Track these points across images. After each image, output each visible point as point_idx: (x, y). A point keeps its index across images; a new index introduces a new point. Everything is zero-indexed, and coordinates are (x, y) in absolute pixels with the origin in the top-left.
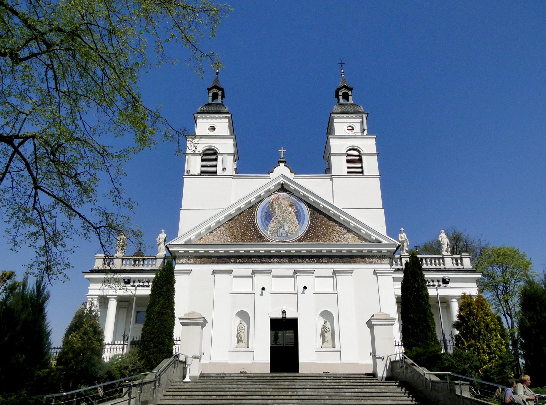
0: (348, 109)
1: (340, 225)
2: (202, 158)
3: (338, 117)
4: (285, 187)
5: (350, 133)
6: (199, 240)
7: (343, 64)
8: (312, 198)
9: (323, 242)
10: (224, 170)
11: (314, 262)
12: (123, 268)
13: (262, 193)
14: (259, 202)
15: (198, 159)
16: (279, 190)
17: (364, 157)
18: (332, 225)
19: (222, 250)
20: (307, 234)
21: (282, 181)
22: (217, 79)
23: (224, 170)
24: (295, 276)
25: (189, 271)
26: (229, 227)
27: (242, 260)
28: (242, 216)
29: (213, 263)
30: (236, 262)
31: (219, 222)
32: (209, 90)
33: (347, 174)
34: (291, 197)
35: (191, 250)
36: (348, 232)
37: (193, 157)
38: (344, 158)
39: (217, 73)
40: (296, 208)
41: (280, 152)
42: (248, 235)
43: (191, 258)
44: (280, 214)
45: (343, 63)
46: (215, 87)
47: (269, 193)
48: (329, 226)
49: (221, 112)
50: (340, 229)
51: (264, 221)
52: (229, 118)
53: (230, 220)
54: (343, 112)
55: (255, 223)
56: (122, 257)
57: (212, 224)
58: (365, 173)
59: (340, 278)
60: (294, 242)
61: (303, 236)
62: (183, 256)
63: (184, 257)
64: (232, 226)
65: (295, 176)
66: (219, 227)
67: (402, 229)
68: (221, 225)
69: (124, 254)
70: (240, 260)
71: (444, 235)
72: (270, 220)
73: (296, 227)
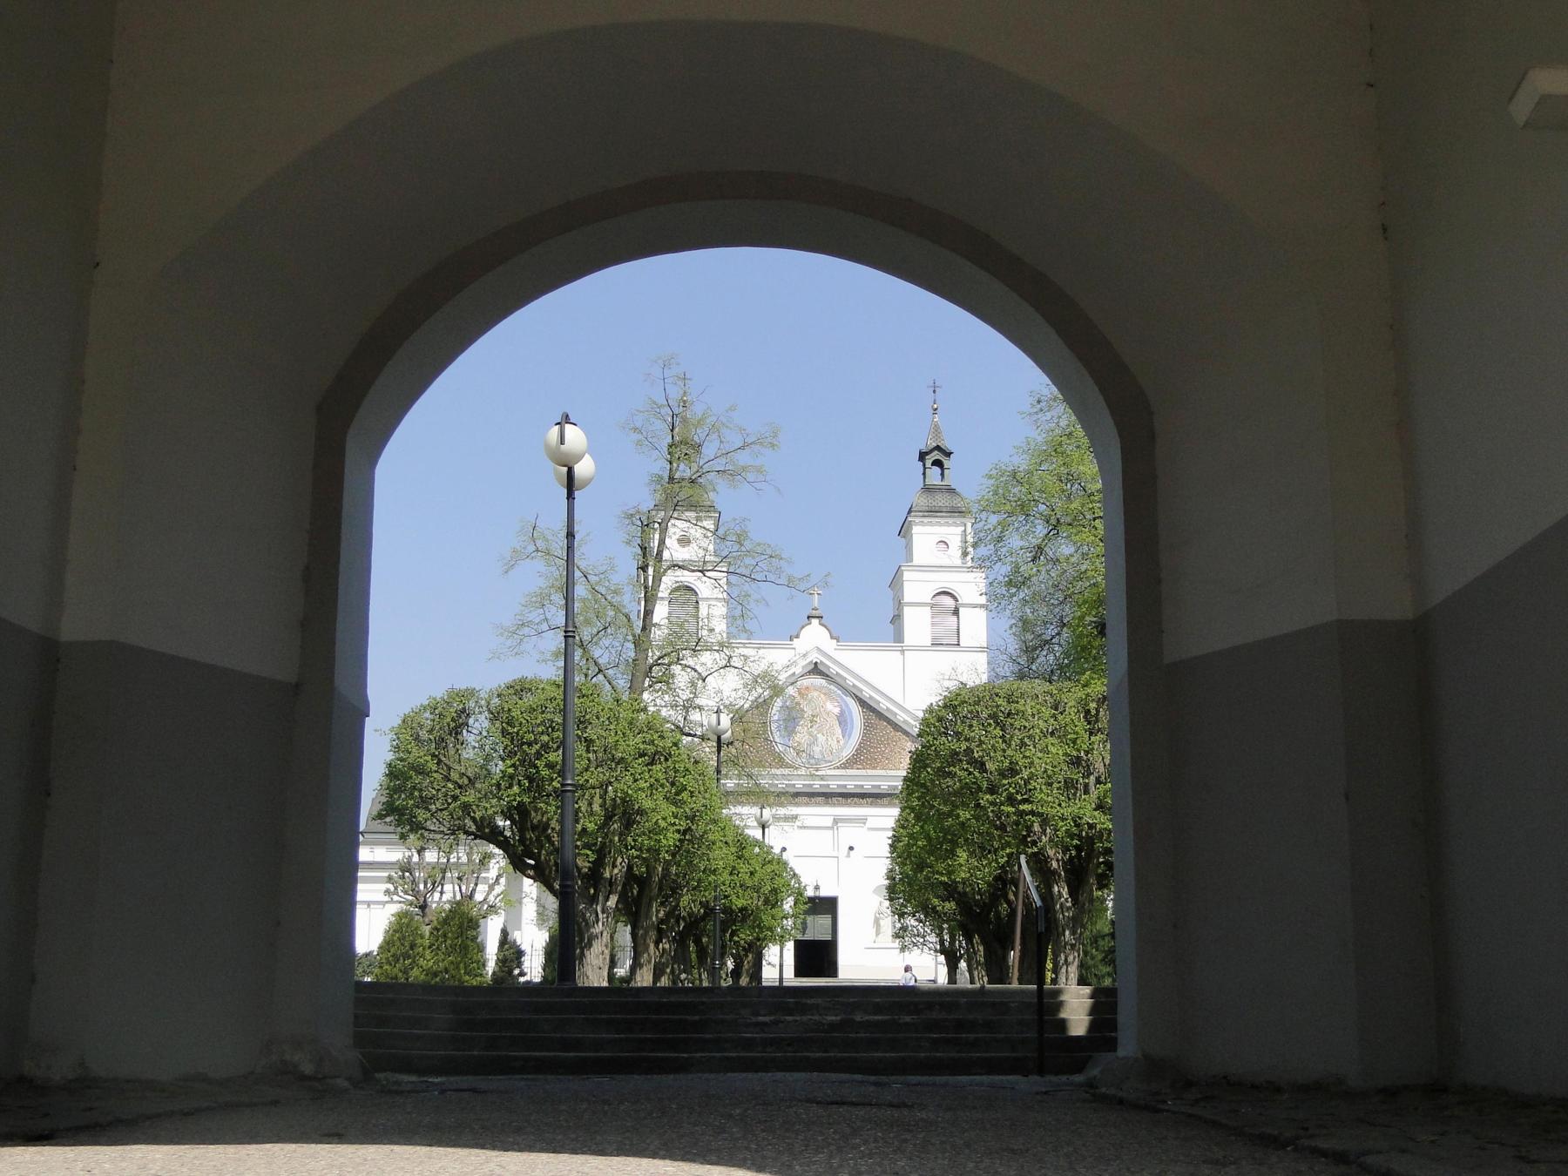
0: (940, 504)
7: (936, 389)
11: (867, 803)
34: (832, 687)
61: (849, 759)
73: (838, 742)
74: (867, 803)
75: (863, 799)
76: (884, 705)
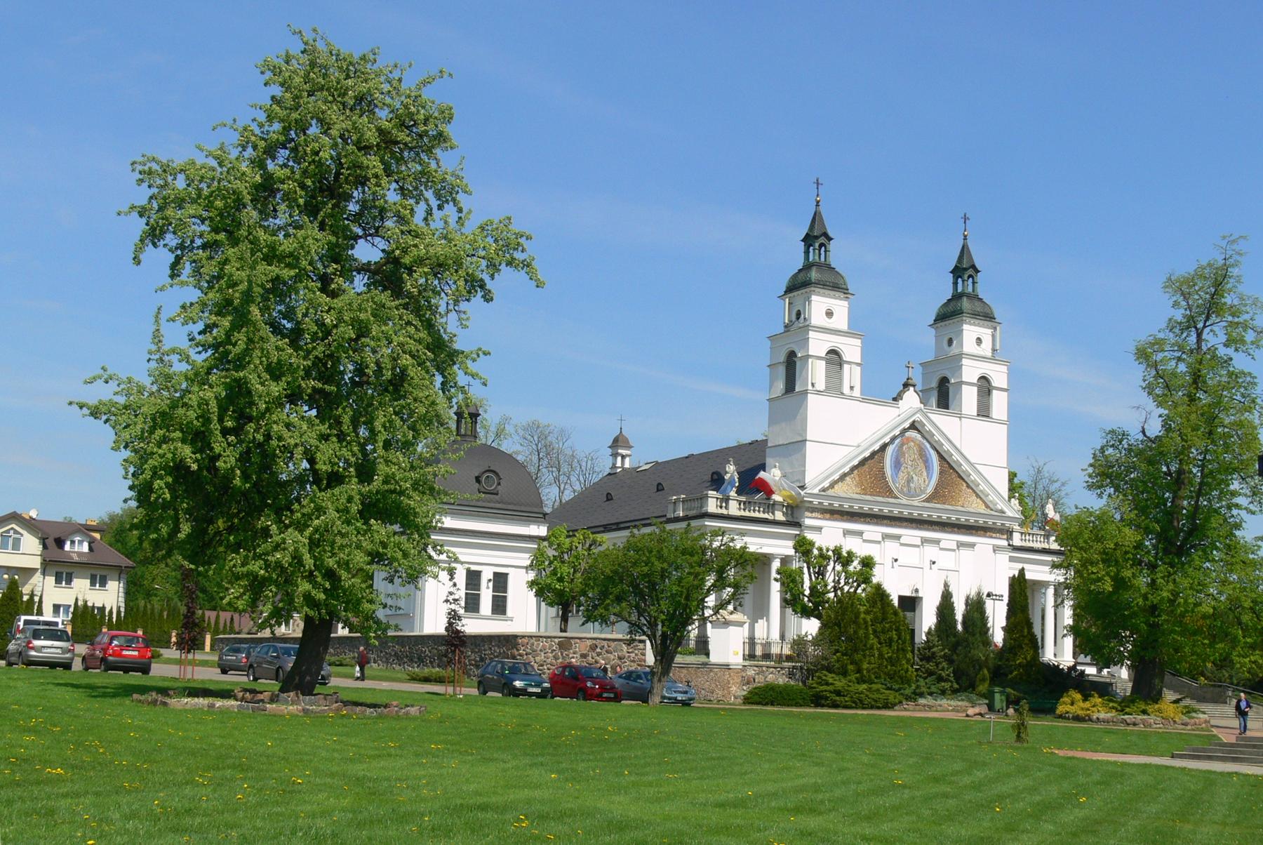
4: (916, 424)
8: (947, 446)
10: (852, 388)
17: (995, 393)
23: (852, 388)
38: (975, 389)
59: (964, 552)
76: (956, 456)
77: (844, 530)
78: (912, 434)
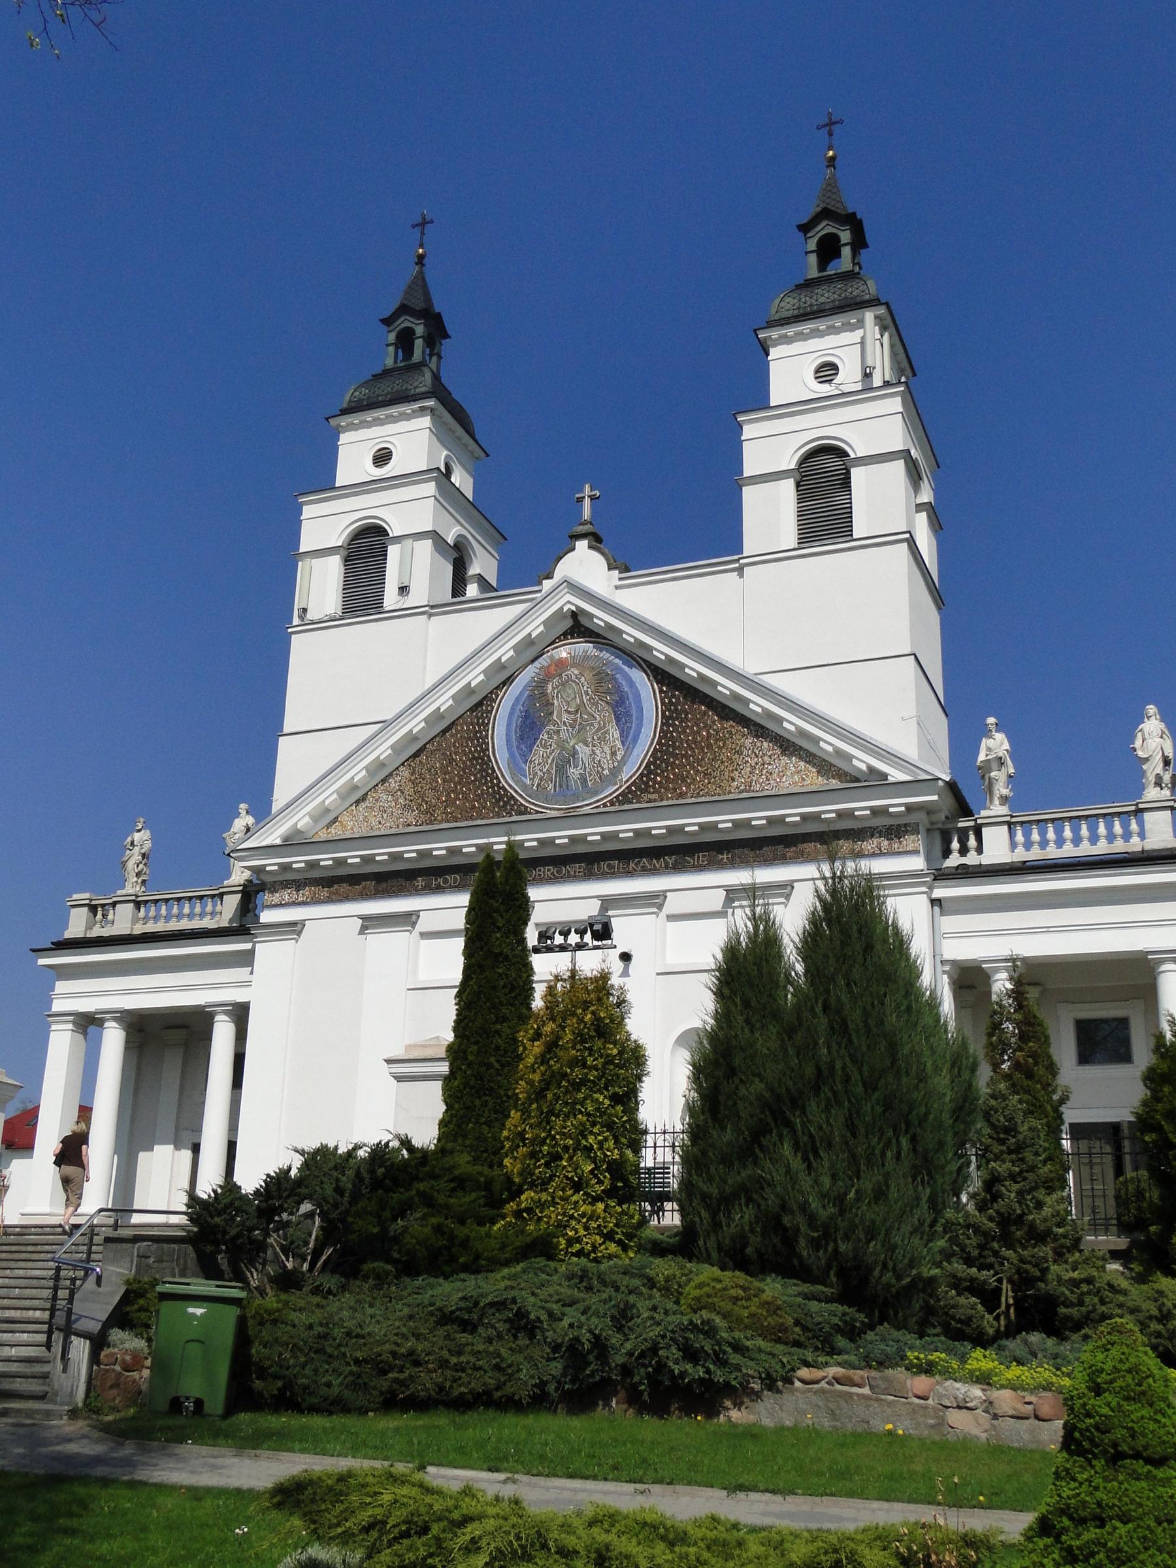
0: (822, 300)
1: (758, 729)
2: (346, 561)
3: (781, 337)
4: (583, 621)
5: (825, 389)
6: (328, 826)
8: (661, 650)
9: (698, 795)
10: (403, 590)
11: (667, 867)
12: (139, 929)
13: (505, 652)
14: (504, 683)
15: (334, 566)
16: (565, 635)
17: (857, 474)
18: (730, 733)
19: (381, 854)
20: (647, 776)
21: (569, 602)
22: (831, 187)
23: (403, 590)
24: (730, 911)
25: (294, 928)
26: (413, 778)
27: (446, 881)
28: (452, 736)
29: (364, 896)
30: (428, 890)
31: (380, 764)
32: (805, 228)
33: (796, 546)
34: (605, 655)
35: (298, 861)
36: (783, 753)
37: (317, 563)
38: (787, 489)
39: (421, 258)
40: (618, 689)
41: (581, 500)
42: (466, 798)
43: (305, 885)
44: (565, 716)
45: (837, 122)
46: (825, 214)
47: (532, 650)
48: (720, 739)
49: (407, 397)
50: (759, 744)
51: (515, 744)
52: (432, 410)
53: (416, 755)
54: (797, 316)
55: (488, 756)
56: (133, 898)
57: (357, 772)
58: (854, 537)
60: (605, 805)
62: (282, 882)
63: (285, 885)
64: (421, 774)
65: (620, 579)
66: (383, 781)
67: (991, 720)
68: (390, 775)
69: (143, 889)
70: (440, 880)
71: (1157, 722)
72: (536, 740)
73: (613, 754)
74: (667, 864)
75: (658, 859)
76: (693, 668)
77: (364, 918)
78: (583, 647)
